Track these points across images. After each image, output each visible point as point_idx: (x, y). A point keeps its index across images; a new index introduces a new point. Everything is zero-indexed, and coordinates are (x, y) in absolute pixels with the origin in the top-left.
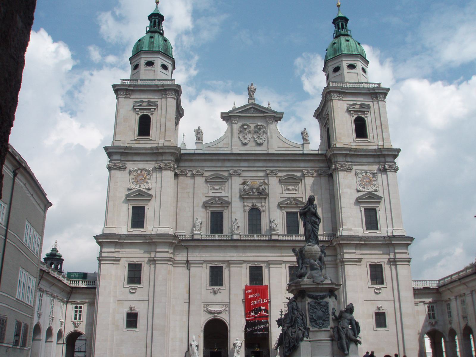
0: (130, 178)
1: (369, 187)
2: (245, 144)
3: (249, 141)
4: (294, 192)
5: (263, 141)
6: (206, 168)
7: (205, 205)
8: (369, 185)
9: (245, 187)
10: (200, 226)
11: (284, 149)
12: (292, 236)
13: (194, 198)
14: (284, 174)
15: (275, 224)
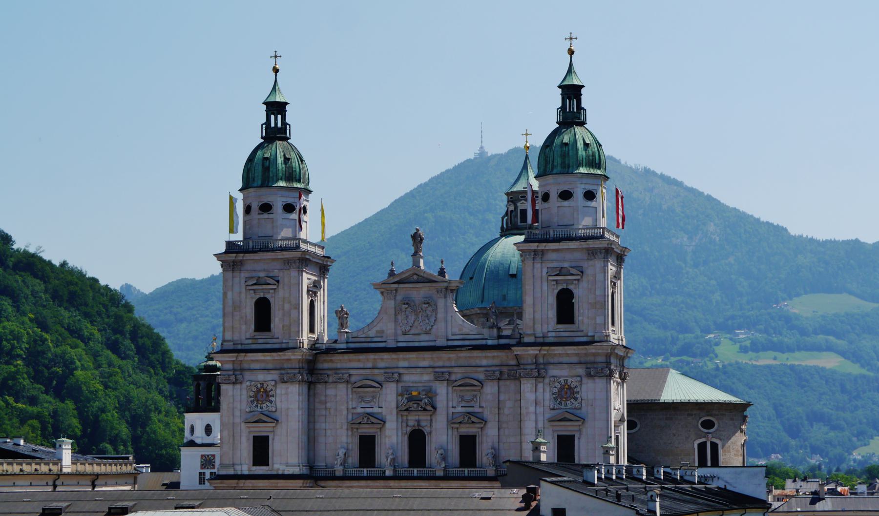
0: (248, 395)
1: (568, 402)
2: (404, 334)
3: (411, 327)
4: (472, 404)
5: (430, 327)
6: (352, 372)
7: (354, 424)
8: (569, 398)
9: (403, 401)
10: (343, 456)
11: (461, 337)
12: (464, 471)
13: (336, 416)
14: (459, 376)
15: (442, 455)
